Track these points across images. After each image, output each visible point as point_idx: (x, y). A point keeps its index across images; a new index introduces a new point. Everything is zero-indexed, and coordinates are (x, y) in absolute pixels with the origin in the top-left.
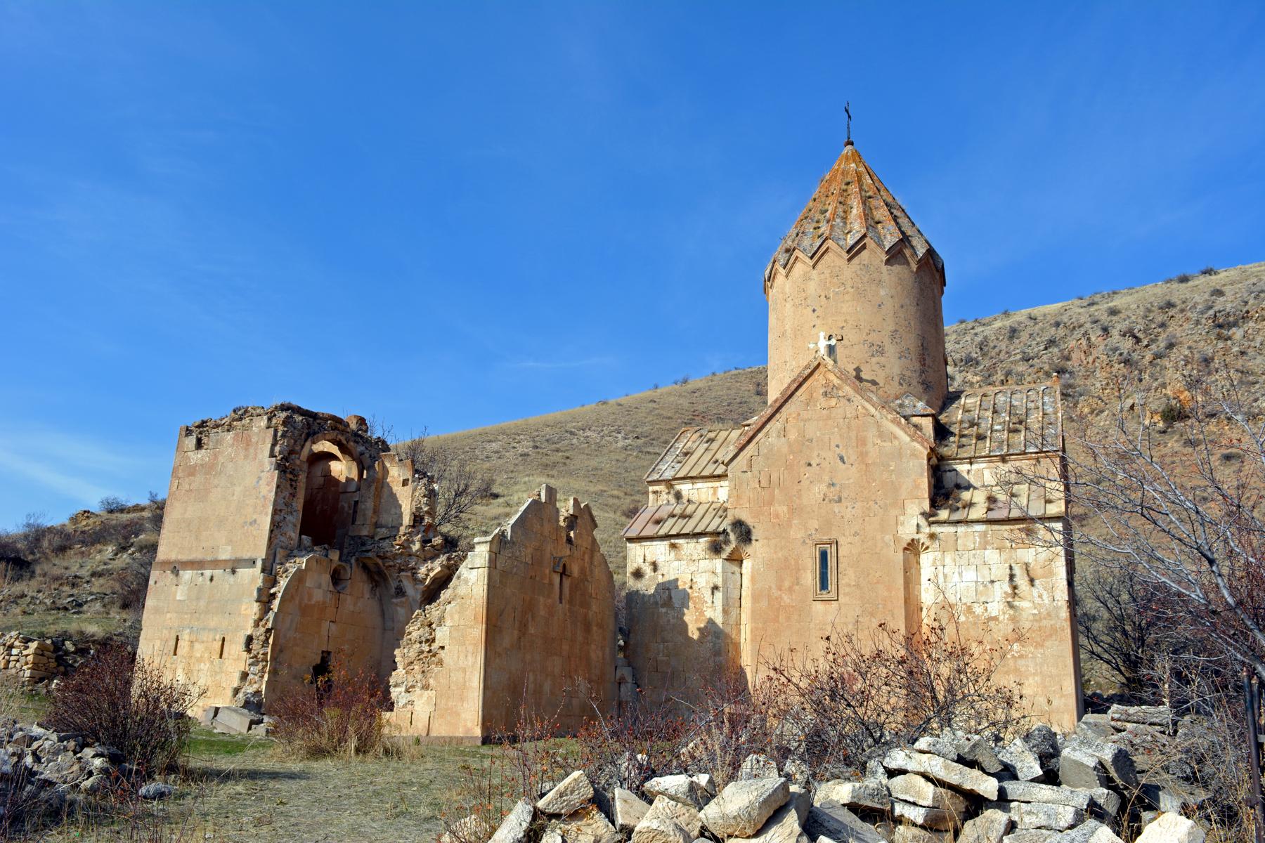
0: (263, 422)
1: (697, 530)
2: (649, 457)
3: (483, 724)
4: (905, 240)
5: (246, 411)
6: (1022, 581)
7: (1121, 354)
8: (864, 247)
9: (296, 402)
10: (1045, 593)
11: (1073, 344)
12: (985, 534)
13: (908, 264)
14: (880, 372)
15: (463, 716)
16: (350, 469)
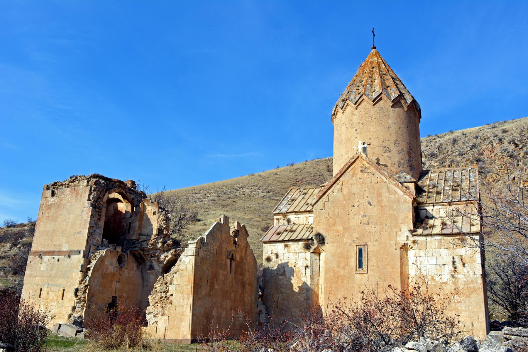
0: (85, 183)
1: (298, 238)
2: (275, 201)
3: (192, 333)
4: (401, 95)
5: (76, 178)
6: (459, 264)
7: (508, 152)
8: (381, 99)
9: (101, 174)
10: (470, 271)
11: (484, 147)
12: (441, 241)
13: (403, 107)
14: (389, 160)
15: (182, 329)
16: (127, 206)
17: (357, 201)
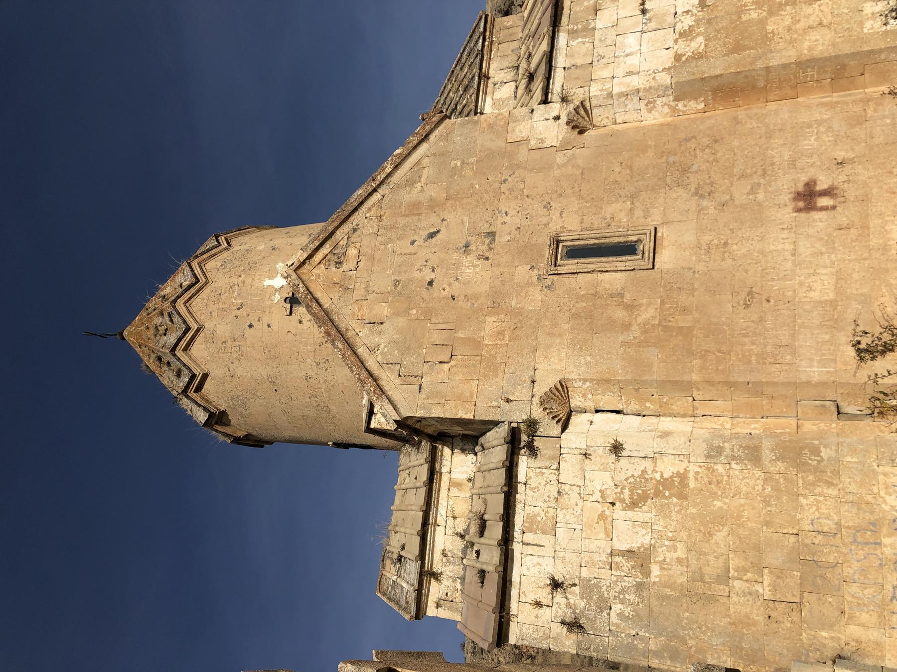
17: (417, 275)
